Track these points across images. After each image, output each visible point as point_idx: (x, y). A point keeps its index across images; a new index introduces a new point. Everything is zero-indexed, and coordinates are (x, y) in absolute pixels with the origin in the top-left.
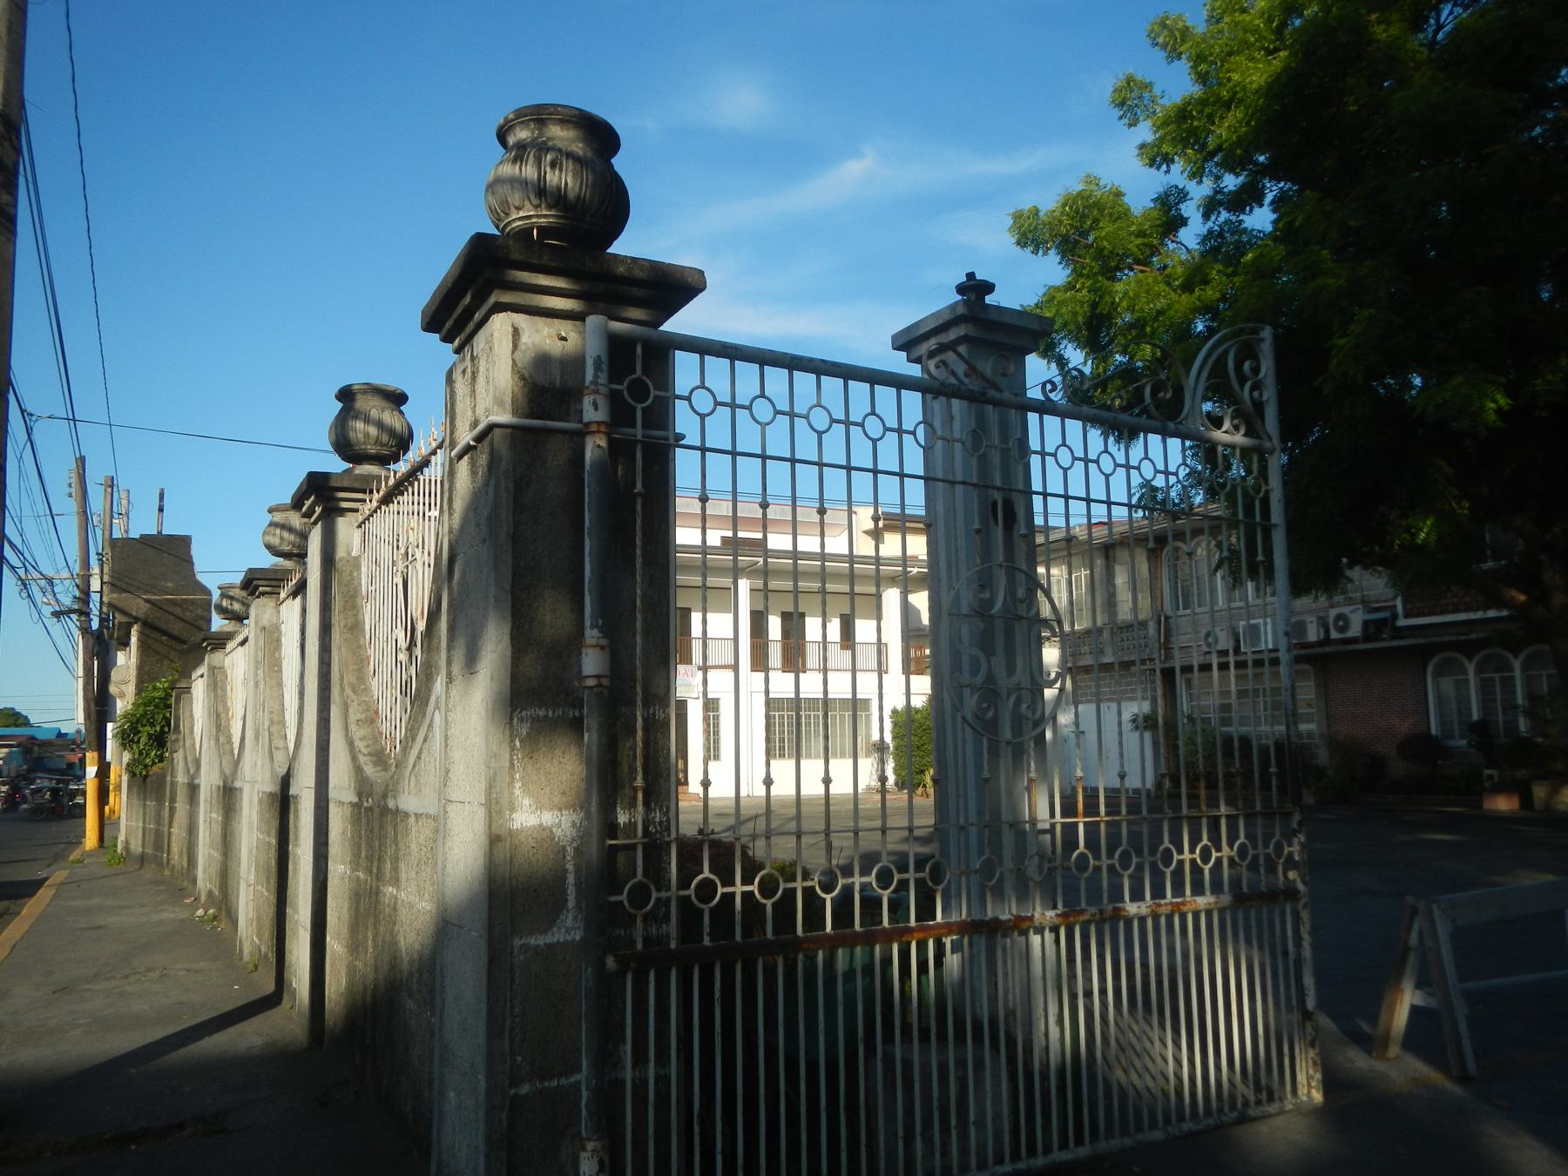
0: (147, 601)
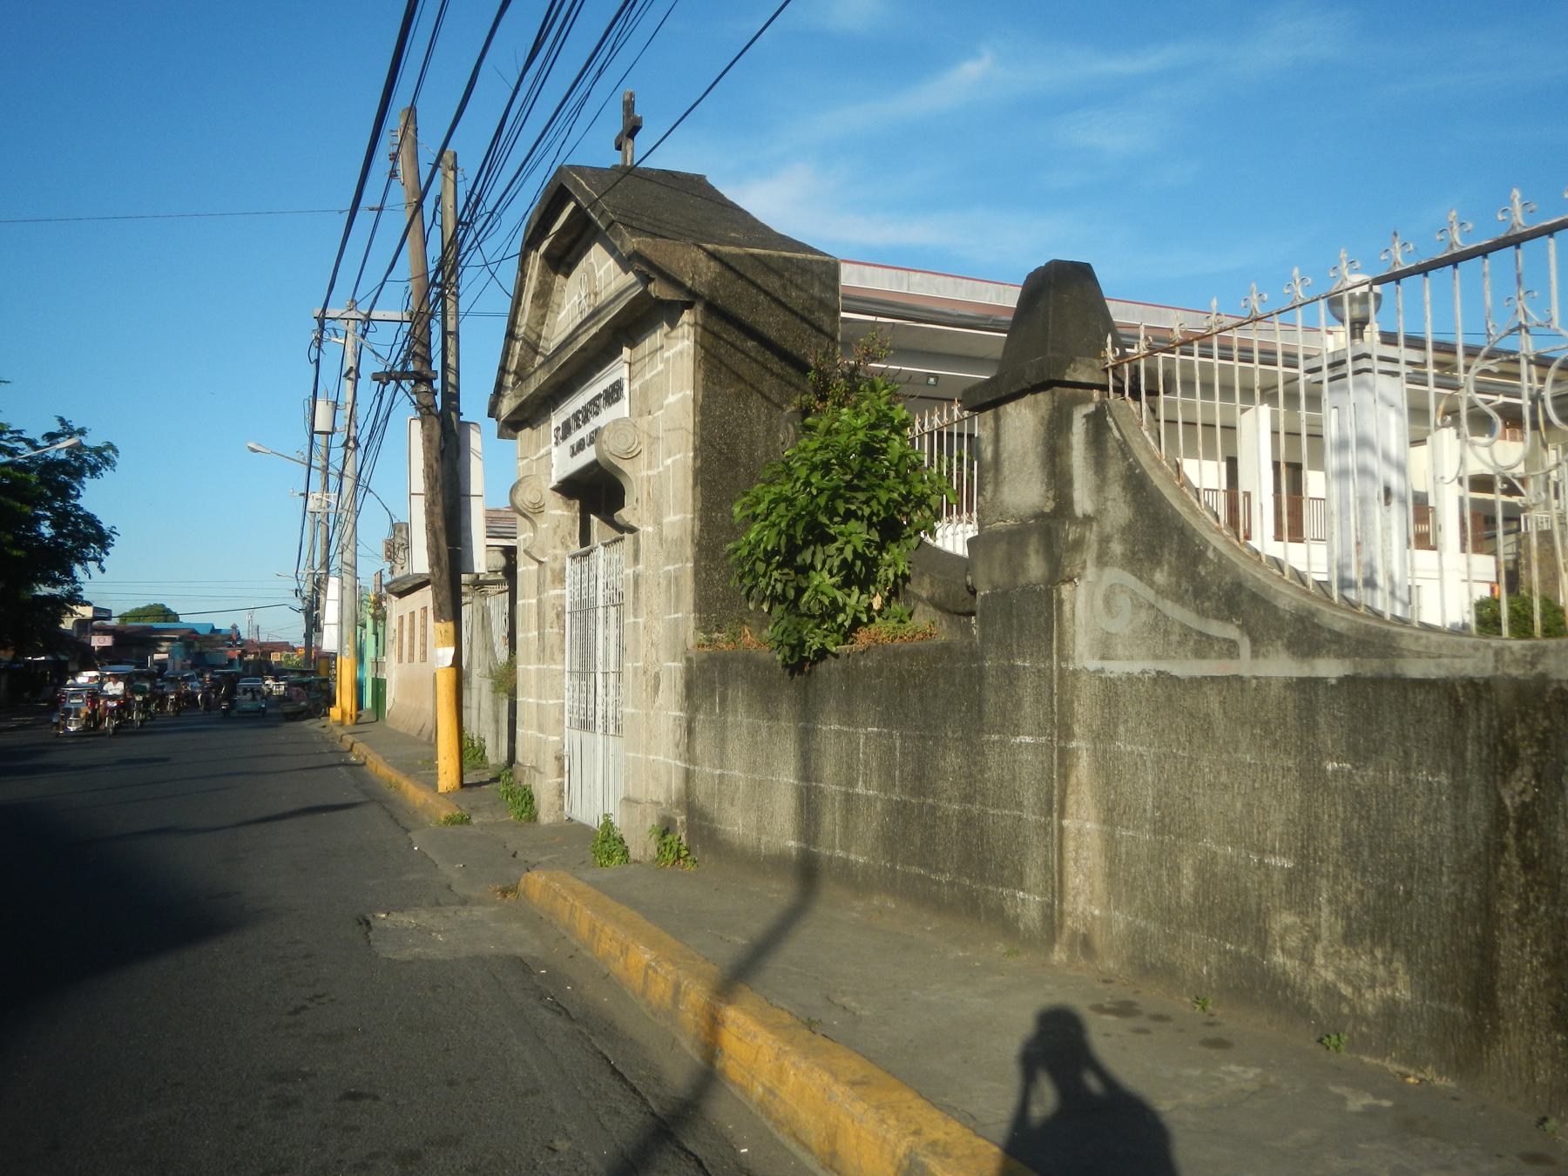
0: (712, 255)
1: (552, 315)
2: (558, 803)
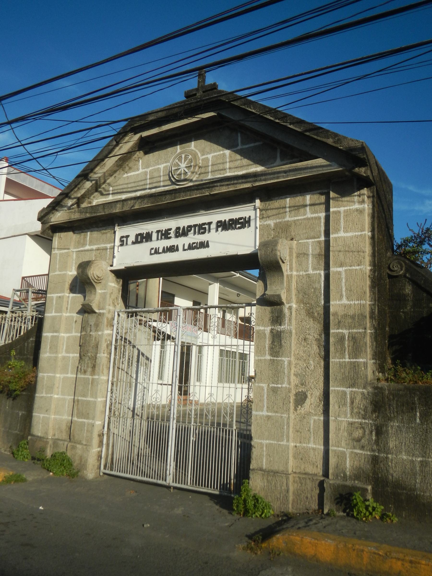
1: (122, 172)
2: (97, 464)
